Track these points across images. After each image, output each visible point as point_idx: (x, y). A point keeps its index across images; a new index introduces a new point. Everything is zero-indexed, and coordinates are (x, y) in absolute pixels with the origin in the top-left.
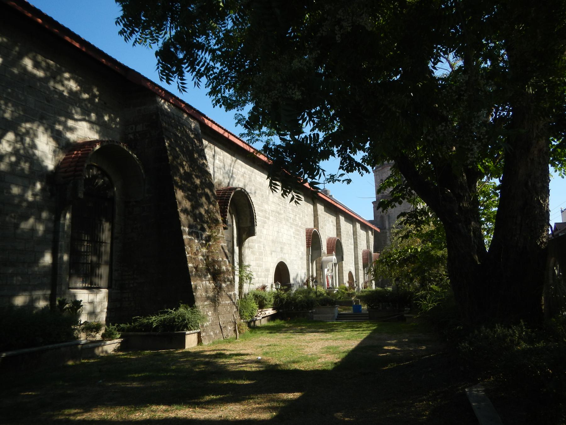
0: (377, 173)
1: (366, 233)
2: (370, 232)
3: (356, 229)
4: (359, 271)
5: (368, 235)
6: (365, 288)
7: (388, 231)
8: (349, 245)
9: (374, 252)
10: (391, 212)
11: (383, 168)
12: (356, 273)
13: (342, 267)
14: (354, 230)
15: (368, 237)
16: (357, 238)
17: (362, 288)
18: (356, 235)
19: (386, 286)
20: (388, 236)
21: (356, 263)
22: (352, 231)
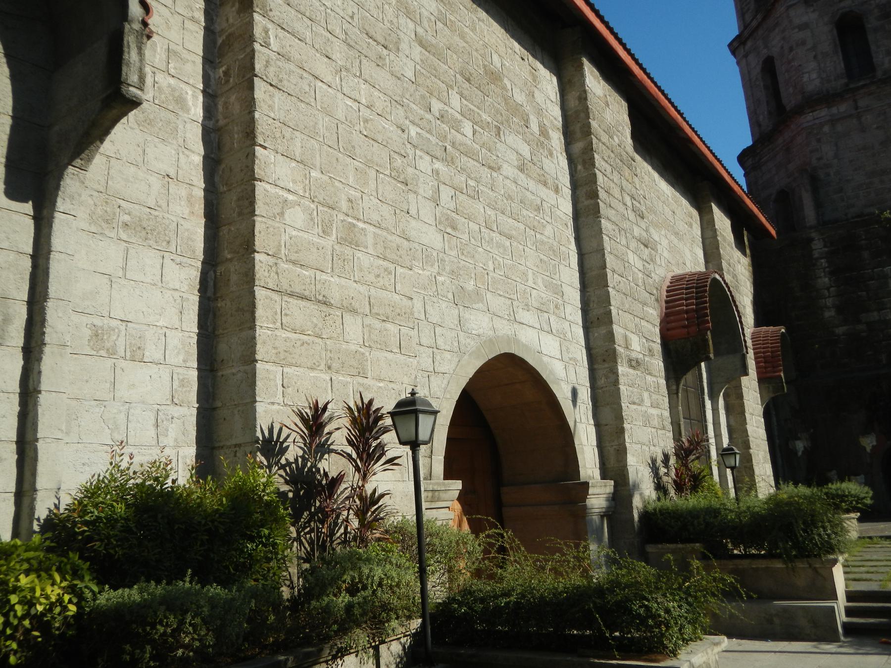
0: (749, 44)
1: (695, 213)
2: (722, 223)
3: (583, 97)
4: (622, 369)
5: (708, 226)
6: (679, 487)
7: (814, 235)
8: (509, 170)
9: (758, 323)
10: (819, 159)
11: (765, 18)
12: (602, 382)
13: (248, 247)
14: (573, 103)
15: (709, 234)
16: (589, 150)
17: (660, 487)
18: (587, 131)
19: (833, 474)
20: (816, 255)
21: (596, 311)
22: (556, 112)
